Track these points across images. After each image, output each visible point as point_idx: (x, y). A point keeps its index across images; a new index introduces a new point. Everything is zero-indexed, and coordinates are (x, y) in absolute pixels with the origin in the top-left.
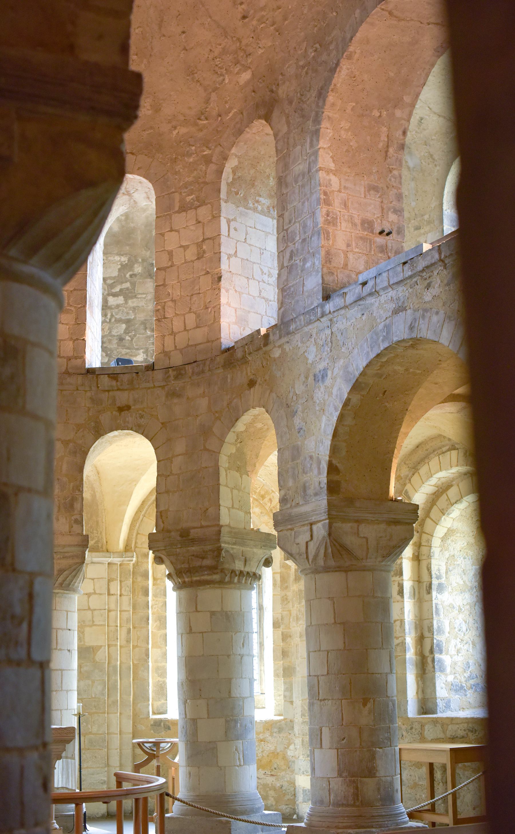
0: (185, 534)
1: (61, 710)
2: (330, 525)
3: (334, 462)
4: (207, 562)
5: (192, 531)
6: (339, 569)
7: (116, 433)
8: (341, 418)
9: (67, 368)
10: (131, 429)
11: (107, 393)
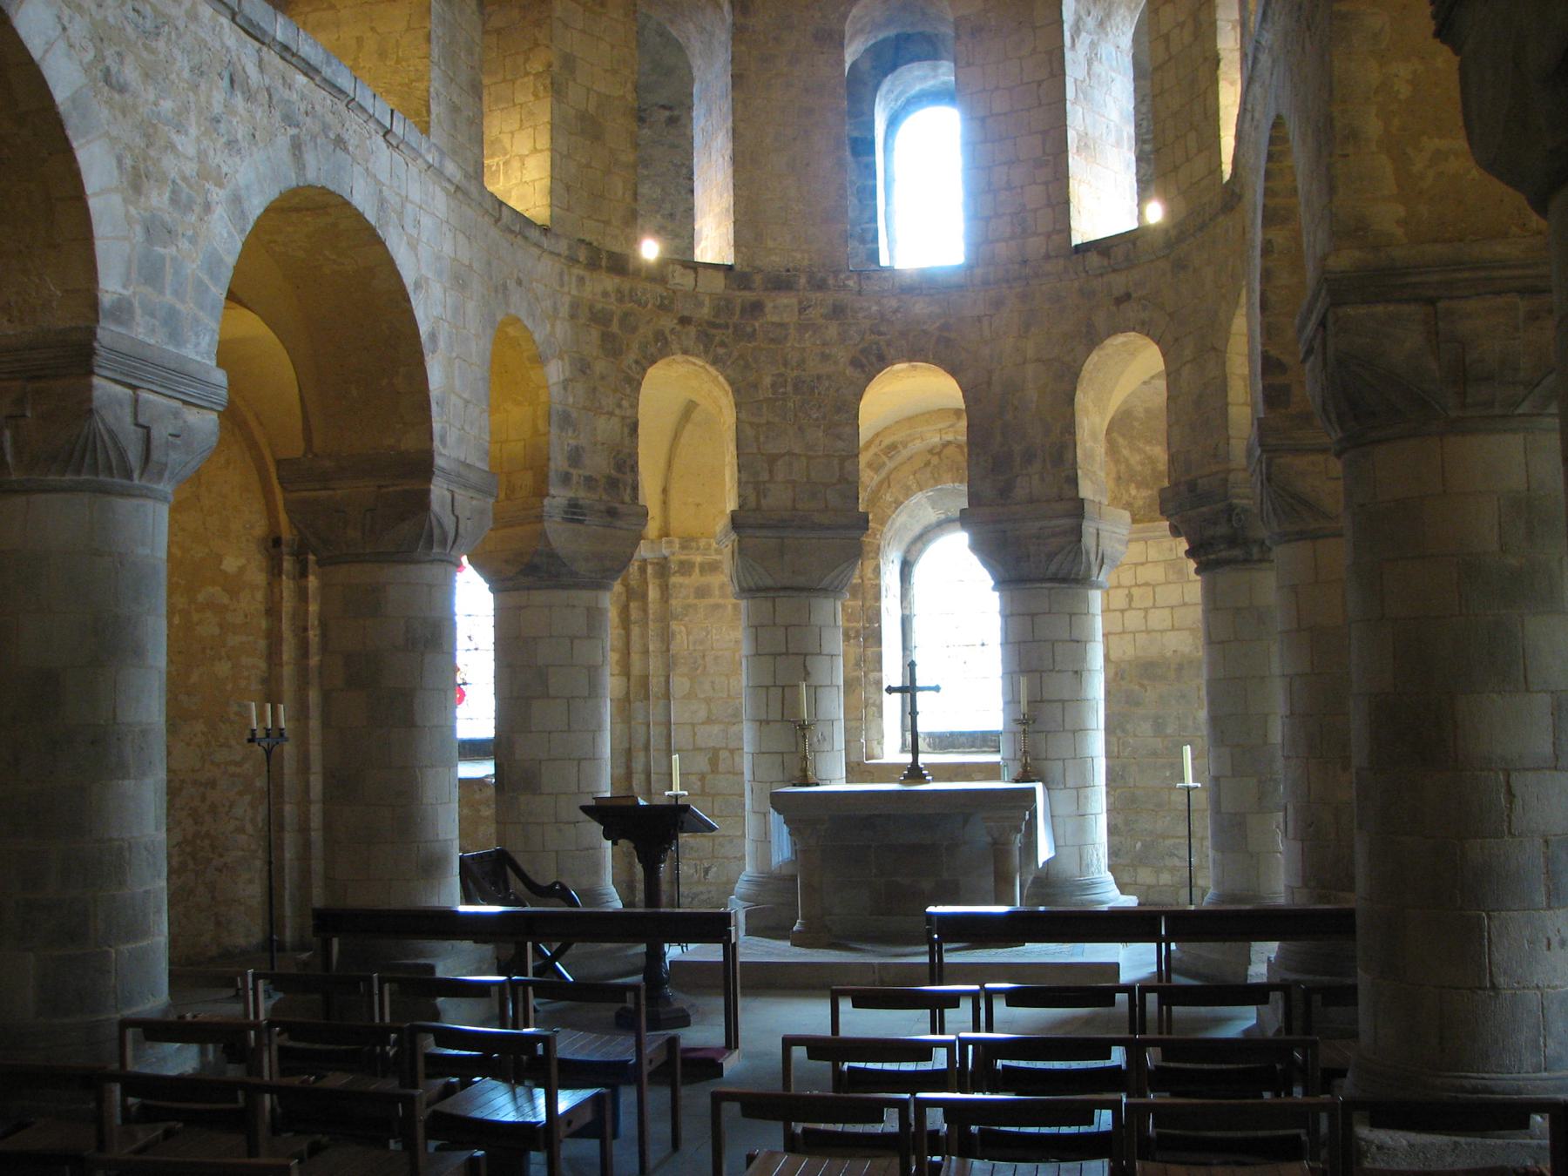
0: (1192, 486)
1: (1064, 760)
2: (1269, 466)
3: (1273, 352)
4: (1222, 530)
5: (1199, 481)
6: (1301, 536)
7: (1120, 339)
8: (1267, 275)
9: (1047, 250)
10: (1134, 330)
11: (1100, 279)
